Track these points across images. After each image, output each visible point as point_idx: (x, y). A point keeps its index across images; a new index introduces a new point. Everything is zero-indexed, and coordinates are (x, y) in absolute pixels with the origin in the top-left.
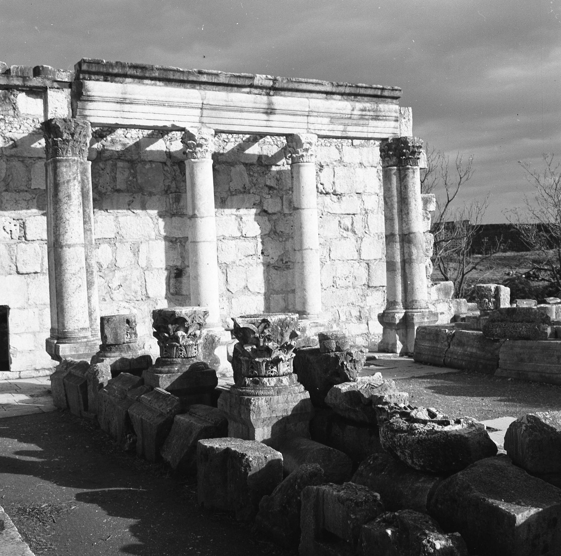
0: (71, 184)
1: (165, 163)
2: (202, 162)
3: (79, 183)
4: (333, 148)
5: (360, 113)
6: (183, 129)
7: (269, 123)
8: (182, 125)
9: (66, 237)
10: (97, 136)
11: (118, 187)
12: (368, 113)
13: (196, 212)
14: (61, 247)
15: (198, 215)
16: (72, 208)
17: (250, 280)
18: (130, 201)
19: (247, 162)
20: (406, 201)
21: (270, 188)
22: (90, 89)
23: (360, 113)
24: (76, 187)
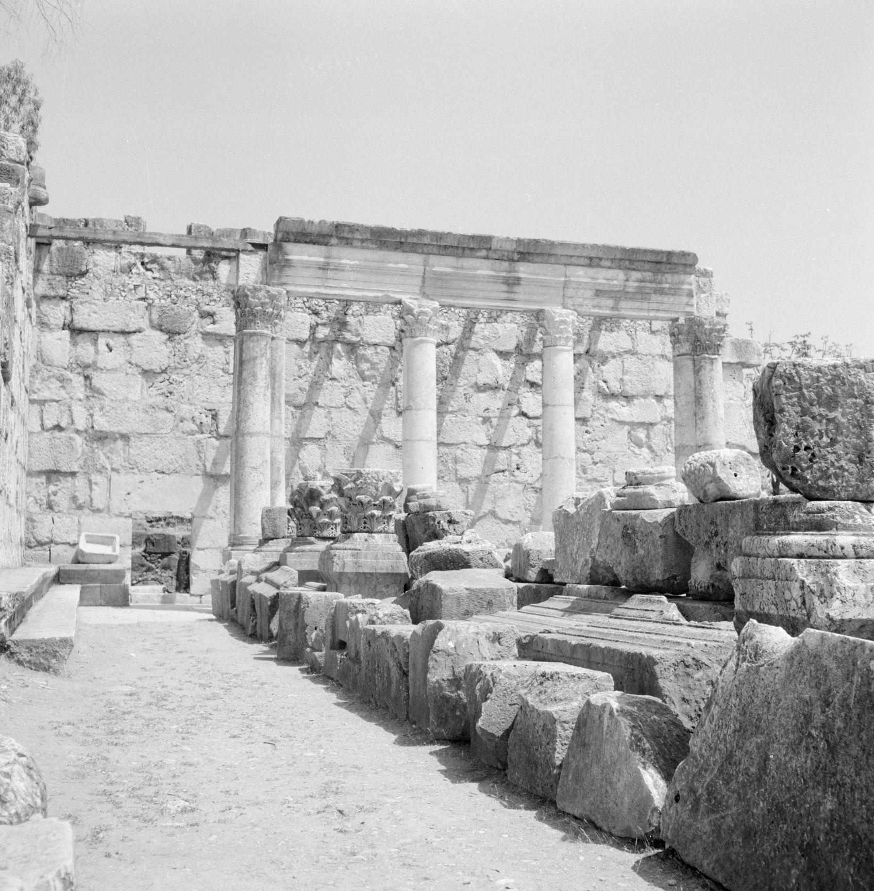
0: (258, 362)
1: (392, 348)
2: (422, 342)
4: (623, 333)
5: (636, 284)
6: (399, 302)
7: (512, 296)
8: (398, 297)
9: (248, 423)
12: (649, 285)
13: (411, 404)
14: (243, 435)
15: (414, 407)
16: (257, 389)
17: (499, 503)
19: (501, 349)
20: (701, 401)
21: (533, 384)
22: (288, 251)
23: (636, 284)
24: (264, 365)
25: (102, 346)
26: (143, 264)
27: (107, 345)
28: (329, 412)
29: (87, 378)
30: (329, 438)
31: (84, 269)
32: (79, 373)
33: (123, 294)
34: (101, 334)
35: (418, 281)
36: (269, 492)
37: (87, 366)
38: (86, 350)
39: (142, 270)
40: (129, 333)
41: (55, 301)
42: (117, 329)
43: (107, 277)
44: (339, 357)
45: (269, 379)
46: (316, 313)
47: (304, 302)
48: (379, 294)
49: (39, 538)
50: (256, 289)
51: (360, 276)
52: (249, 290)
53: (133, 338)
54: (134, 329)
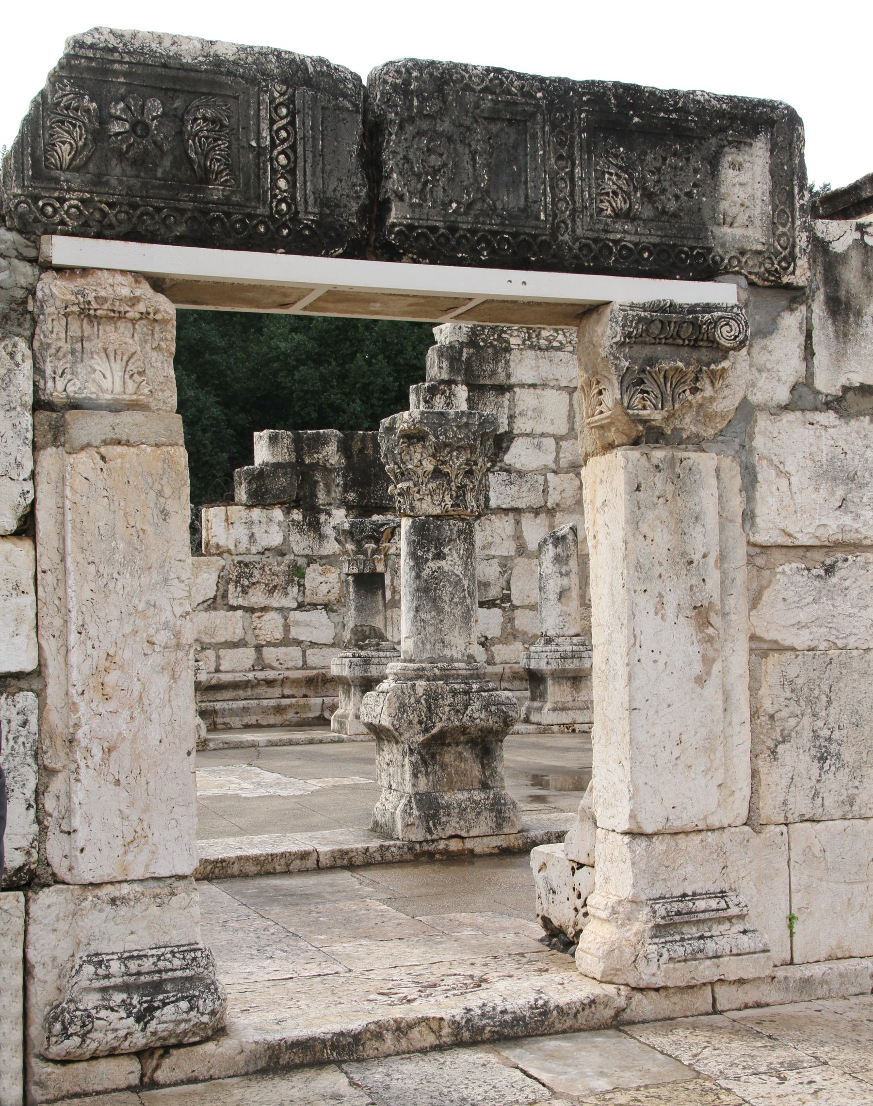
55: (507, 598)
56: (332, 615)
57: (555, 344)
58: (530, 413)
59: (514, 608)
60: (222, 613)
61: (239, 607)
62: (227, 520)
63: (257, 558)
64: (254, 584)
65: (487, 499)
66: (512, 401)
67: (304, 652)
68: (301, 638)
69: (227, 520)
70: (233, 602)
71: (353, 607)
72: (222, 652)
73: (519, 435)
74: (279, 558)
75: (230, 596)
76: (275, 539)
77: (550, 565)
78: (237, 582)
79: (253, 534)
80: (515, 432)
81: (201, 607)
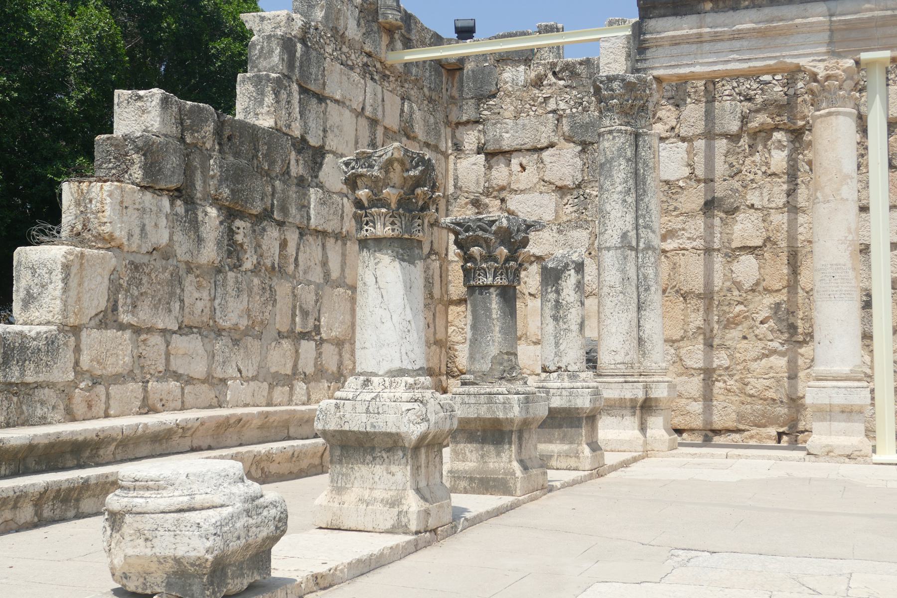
2: (830, 114)
3: (628, 160)
8: (795, 61)
10: (742, 98)
11: (773, 169)
18: (790, 190)
24: (622, 167)
25: (515, 167)
26: (554, 74)
27: (521, 165)
28: (769, 214)
29: (503, 200)
30: (769, 245)
31: (493, 89)
32: (495, 197)
33: (534, 108)
34: (515, 154)
35: (825, 36)
36: (635, 315)
37: (503, 189)
38: (500, 174)
39: (553, 80)
40: (542, 149)
41: (469, 126)
42: (528, 146)
43: (518, 93)
44: (780, 146)
45: (631, 182)
46: (749, 99)
47: (734, 88)
48: (772, 62)
49: (460, 368)
50: (610, 79)
51: (745, 43)
52: (601, 82)
53: (545, 155)
54: (545, 145)
55: (317, 329)
56: (206, 340)
57: (350, 63)
58: (335, 130)
59: (322, 341)
60: (110, 333)
61: (130, 326)
62: (122, 202)
63: (146, 259)
64: (142, 294)
65: (309, 219)
66: (324, 113)
67: (183, 389)
68: (181, 371)
69: (122, 202)
70: (125, 318)
71: (497, 329)
72: (113, 389)
73: (329, 152)
74: (164, 262)
75: (120, 309)
76: (161, 237)
77: (572, 293)
78: (127, 291)
79: (144, 225)
80: (327, 148)
81: (93, 323)
